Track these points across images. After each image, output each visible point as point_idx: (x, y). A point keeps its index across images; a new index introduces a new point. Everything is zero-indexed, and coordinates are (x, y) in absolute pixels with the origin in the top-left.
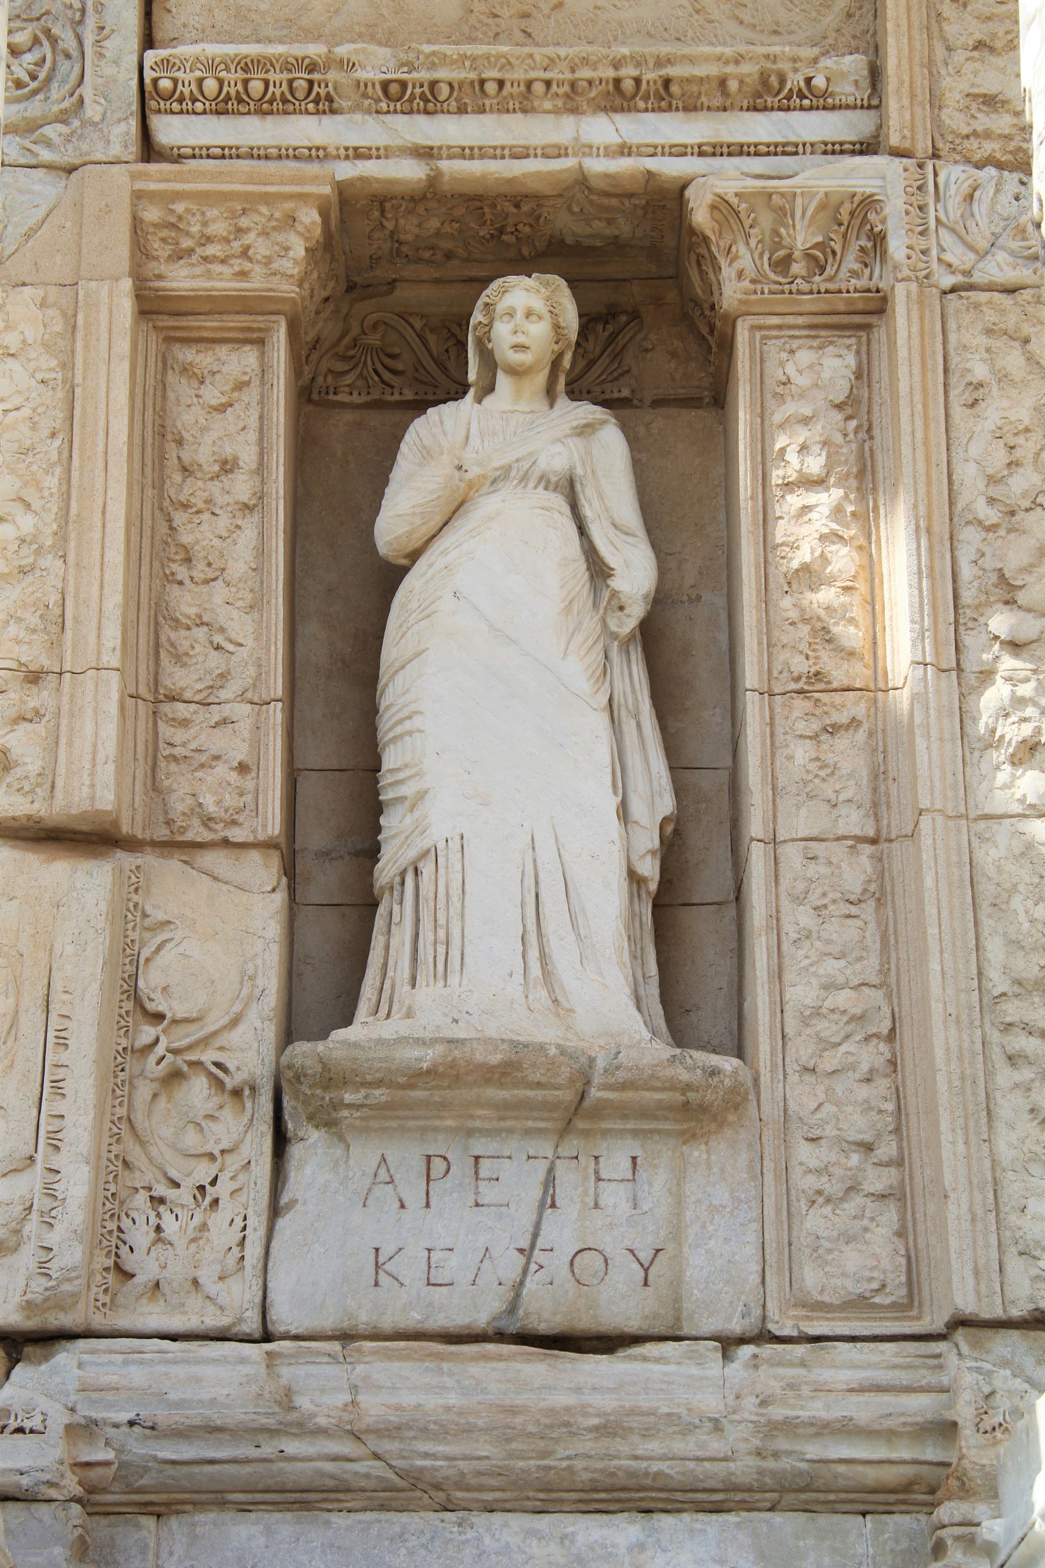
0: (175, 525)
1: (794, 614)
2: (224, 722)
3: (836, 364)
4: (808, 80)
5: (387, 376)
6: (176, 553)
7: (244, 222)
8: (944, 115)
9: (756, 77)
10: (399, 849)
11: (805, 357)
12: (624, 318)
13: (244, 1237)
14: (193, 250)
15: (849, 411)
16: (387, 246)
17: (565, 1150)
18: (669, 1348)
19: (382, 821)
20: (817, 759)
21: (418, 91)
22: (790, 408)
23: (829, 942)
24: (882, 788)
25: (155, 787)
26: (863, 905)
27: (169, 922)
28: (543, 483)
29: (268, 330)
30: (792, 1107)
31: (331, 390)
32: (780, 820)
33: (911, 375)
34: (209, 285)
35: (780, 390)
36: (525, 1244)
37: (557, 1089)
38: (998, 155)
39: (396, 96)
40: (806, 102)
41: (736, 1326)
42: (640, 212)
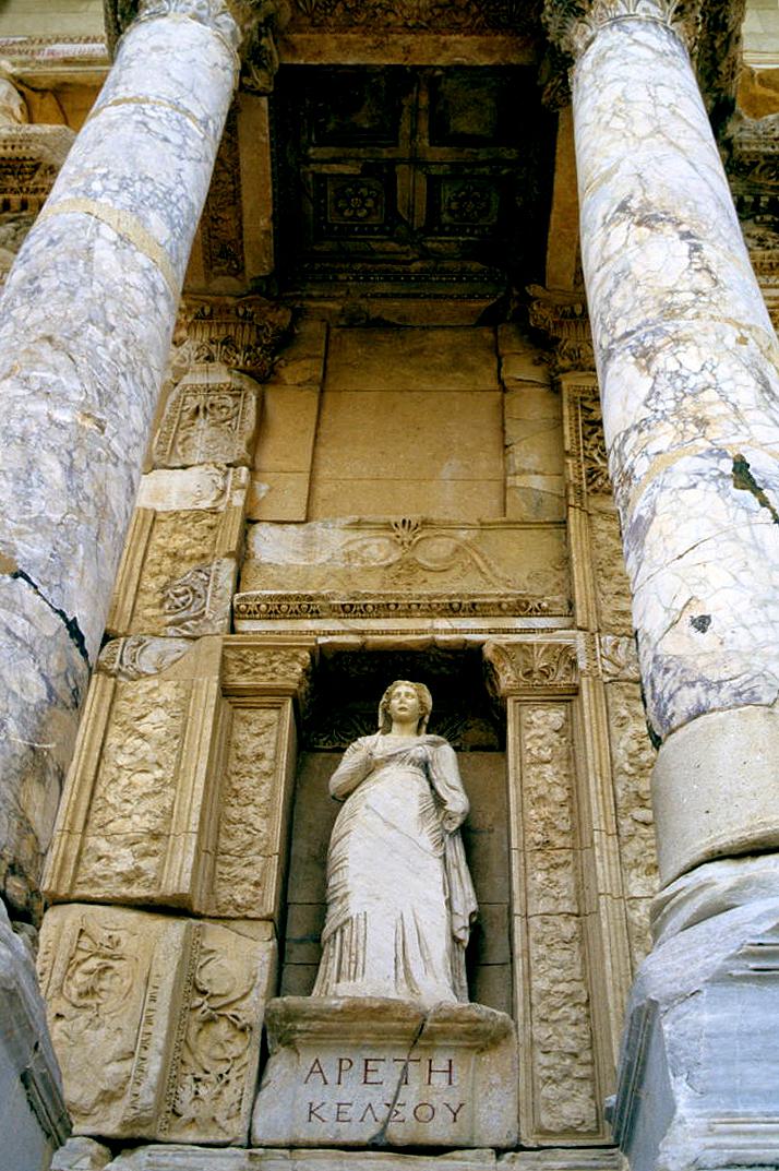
1: (536, 817)
3: (556, 716)
7: (274, 658)
11: (541, 713)
18: (466, 1153)
22: (533, 732)
39: (347, 611)
41: (504, 1143)
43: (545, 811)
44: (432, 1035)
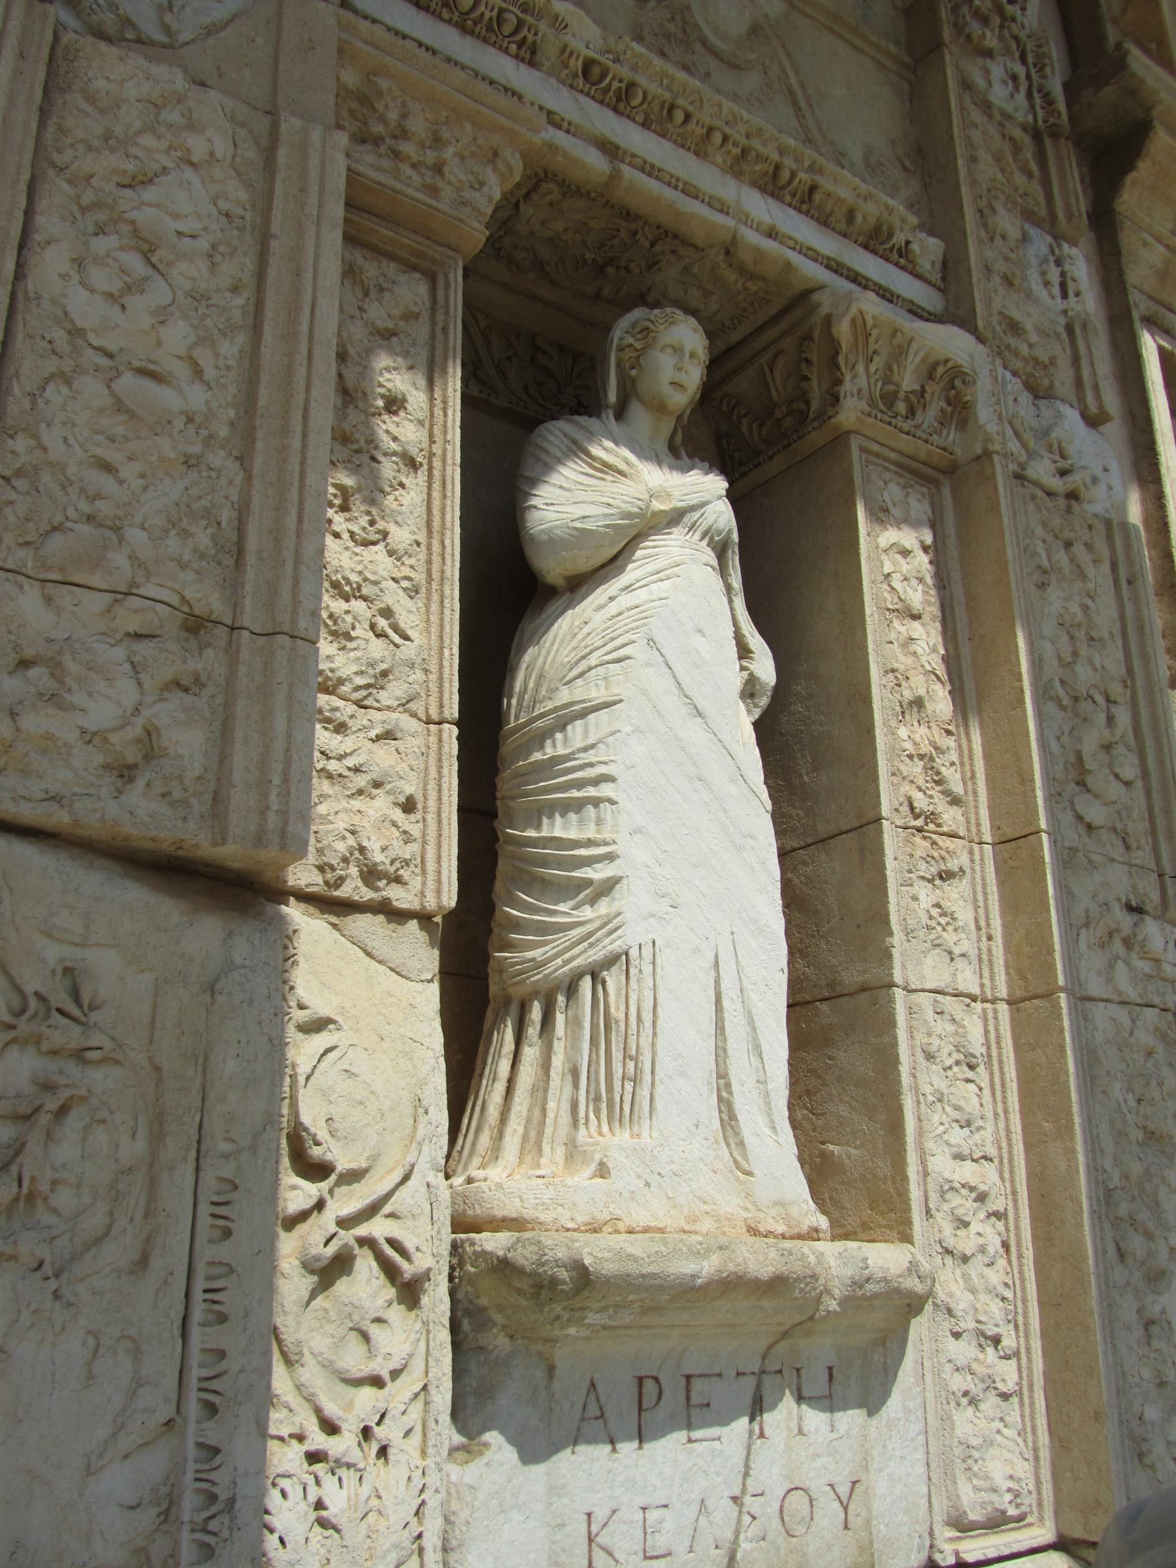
2: (388, 735)
4: (908, 243)
9: (872, 221)
13: (423, 1502)
14: (382, 139)
20: (938, 905)
21: (616, 85)
23: (957, 1108)
36: (737, 1491)
40: (902, 261)
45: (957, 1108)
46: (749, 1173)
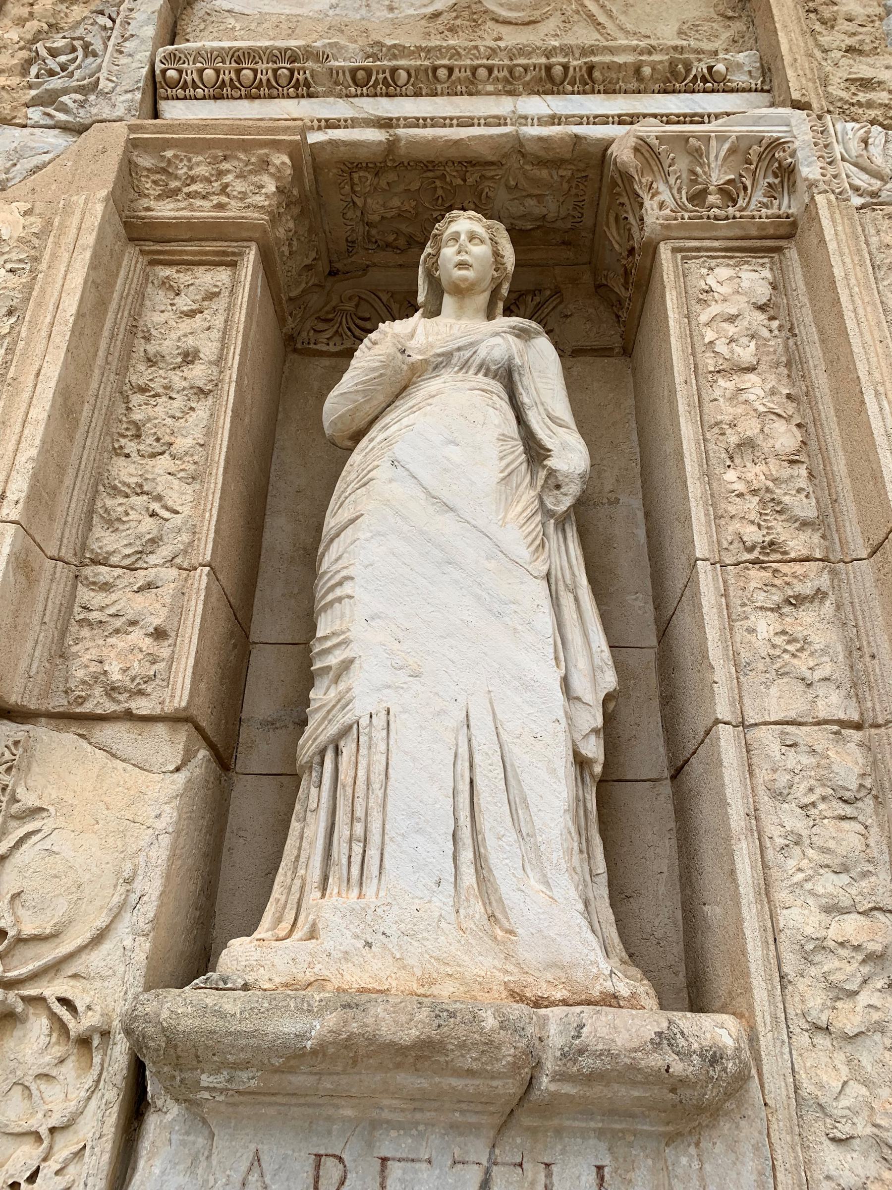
0: (130, 405)
1: (740, 487)
3: (755, 279)
4: (710, 68)
5: (358, 332)
6: (127, 429)
7: (225, 166)
8: (830, 89)
10: (319, 725)
11: (723, 272)
12: (548, 293)
15: (772, 313)
16: (361, 229)
17: (507, 1154)
19: (312, 695)
20: (784, 632)
21: (381, 76)
22: (715, 309)
23: (824, 850)
24: (860, 666)
25: (61, 654)
26: (860, 804)
27: (41, 809)
28: (483, 371)
29: (241, 254)
30: (807, 1087)
31: (313, 341)
32: (746, 700)
33: (844, 263)
34: (189, 214)
35: (704, 296)
37: (493, 1078)
38: (881, 119)
42: (565, 186)
43: (756, 473)
44: (551, 1107)
45: (824, 850)
46: (511, 932)
